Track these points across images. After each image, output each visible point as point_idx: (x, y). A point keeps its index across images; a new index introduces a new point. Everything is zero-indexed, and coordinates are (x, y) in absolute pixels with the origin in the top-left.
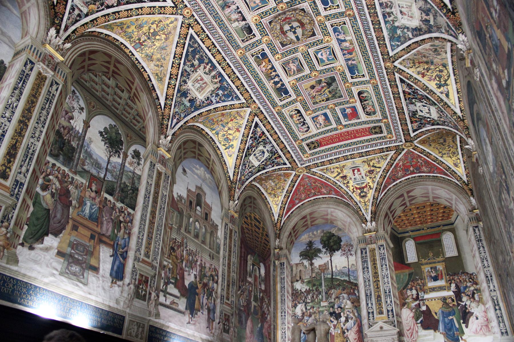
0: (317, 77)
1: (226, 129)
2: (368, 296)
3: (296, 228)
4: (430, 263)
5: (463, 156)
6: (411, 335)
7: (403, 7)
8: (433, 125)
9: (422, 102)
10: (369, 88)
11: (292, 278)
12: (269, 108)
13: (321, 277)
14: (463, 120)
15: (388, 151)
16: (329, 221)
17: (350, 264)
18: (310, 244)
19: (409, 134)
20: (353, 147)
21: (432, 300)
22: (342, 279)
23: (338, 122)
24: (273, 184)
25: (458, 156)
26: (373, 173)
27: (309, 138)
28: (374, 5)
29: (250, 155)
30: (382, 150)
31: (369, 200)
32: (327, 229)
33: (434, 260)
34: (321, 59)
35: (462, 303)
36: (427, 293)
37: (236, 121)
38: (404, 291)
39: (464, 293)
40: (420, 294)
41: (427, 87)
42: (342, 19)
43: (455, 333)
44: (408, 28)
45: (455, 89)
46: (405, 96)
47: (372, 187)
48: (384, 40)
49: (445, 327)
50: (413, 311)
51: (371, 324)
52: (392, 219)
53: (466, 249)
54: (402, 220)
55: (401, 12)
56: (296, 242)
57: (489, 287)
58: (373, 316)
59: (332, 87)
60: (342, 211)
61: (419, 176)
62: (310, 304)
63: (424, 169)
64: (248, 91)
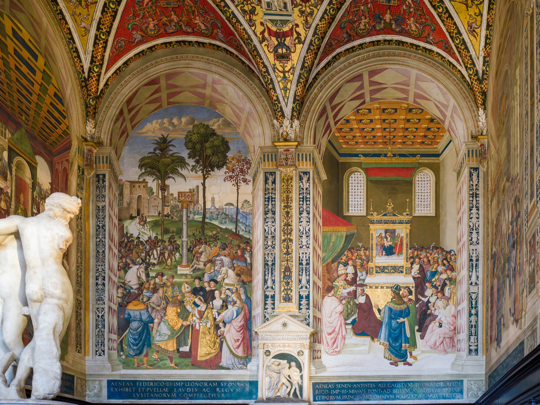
2: (269, 267)
3: (134, 103)
4: (386, 222)
11: (120, 210)
13: (182, 216)
16: (207, 102)
17: (241, 200)
21: (376, 287)
22: (223, 227)
32: (200, 118)
33: (394, 218)
35: (423, 299)
36: (371, 273)
39: (430, 282)
40: (359, 274)
43: (403, 345)
51: (267, 316)
54: (351, 129)
57: (470, 277)
58: (274, 304)
62: (157, 268)
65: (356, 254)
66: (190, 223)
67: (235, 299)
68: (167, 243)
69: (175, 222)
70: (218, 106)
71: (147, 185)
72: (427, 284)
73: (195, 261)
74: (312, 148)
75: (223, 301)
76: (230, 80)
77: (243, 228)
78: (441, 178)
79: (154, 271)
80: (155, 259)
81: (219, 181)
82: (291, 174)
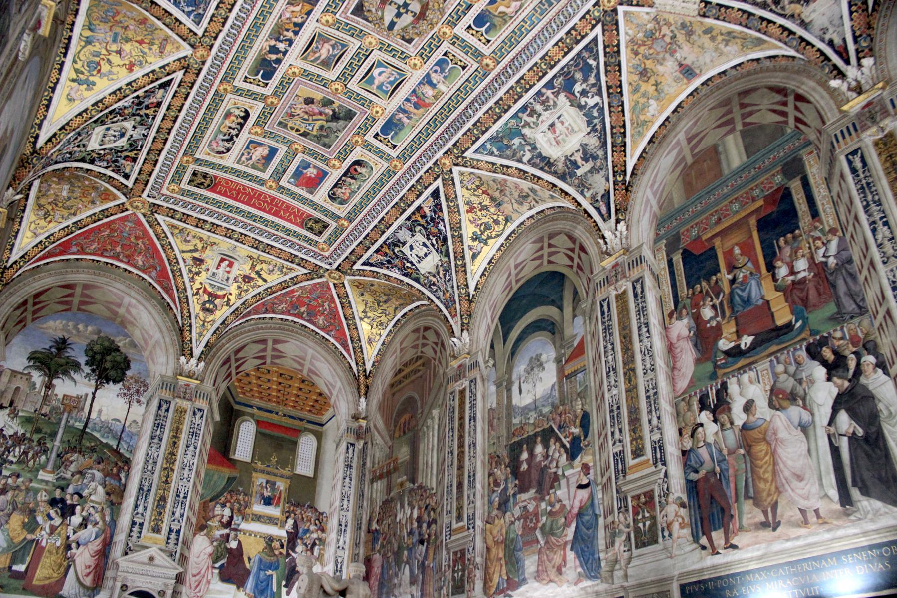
0: (335, 94)
1: (114, 47)
3: (42, 298)
4: (268, 473)
5: (388, 335)
6: (197, 586)
7: (562, 123)
8: (406, 275)
9: (428, 239)
10: (379, 167)
12: (215, 76)
13: (61, 419)
14: (471, 302)
15: (299, 265)
16: (119, 320)
18: (62, 344)
19: (355, 263)
20: (258, 225)
21: (250, 535)
22: (104, 441)
23: (278, 175)
24: (65, 194)
25: (382, 332)
26: (248, 282)
27: (212, 165)
28: (531, 87)
29: (103, 123)
30: (291, 258)
31: (214, 321)
32: (108, 331)
34: (373, 78)
35: (293, 554)
36: (247, 520)
37: (146, 50)
38: (212, 504)
39: (302, 539)
40: (235, 518)
41: (460, 228)
42: (469, 59)
44: (534, 148)
45: (490, 256)
46: (413, 213)
47: (231, 303)
48: (483, 133)
49: (256, 585)
50: (215, 543)
51: (130, 545)
52: (234, 373)
53: (327, 472)
54: (250, 383)
55: (552, 125)
56: (30, 325)
57: (338, 541)
58: (140, 533)
59: (333, 125)
60: (150, 313)
61: (303, 326)
62: (14, 467)
63: (321, 320)
64: (224, 24)
65: (235, 498)
66: (69, 428)
67: (98, 519)
68: (35, 443)
69: (53, 423)
70: (128, 327)
71: (30, 379)
72: (299, 540)
73: (62, 469)
74: (210, 389)
75: (84, 519)
76: (146, 309)
77: (125, 446)
78: (323, 444)
79: (9, 470)
80: (15, 457)
81: (111, 395)
82: (186, 407)
